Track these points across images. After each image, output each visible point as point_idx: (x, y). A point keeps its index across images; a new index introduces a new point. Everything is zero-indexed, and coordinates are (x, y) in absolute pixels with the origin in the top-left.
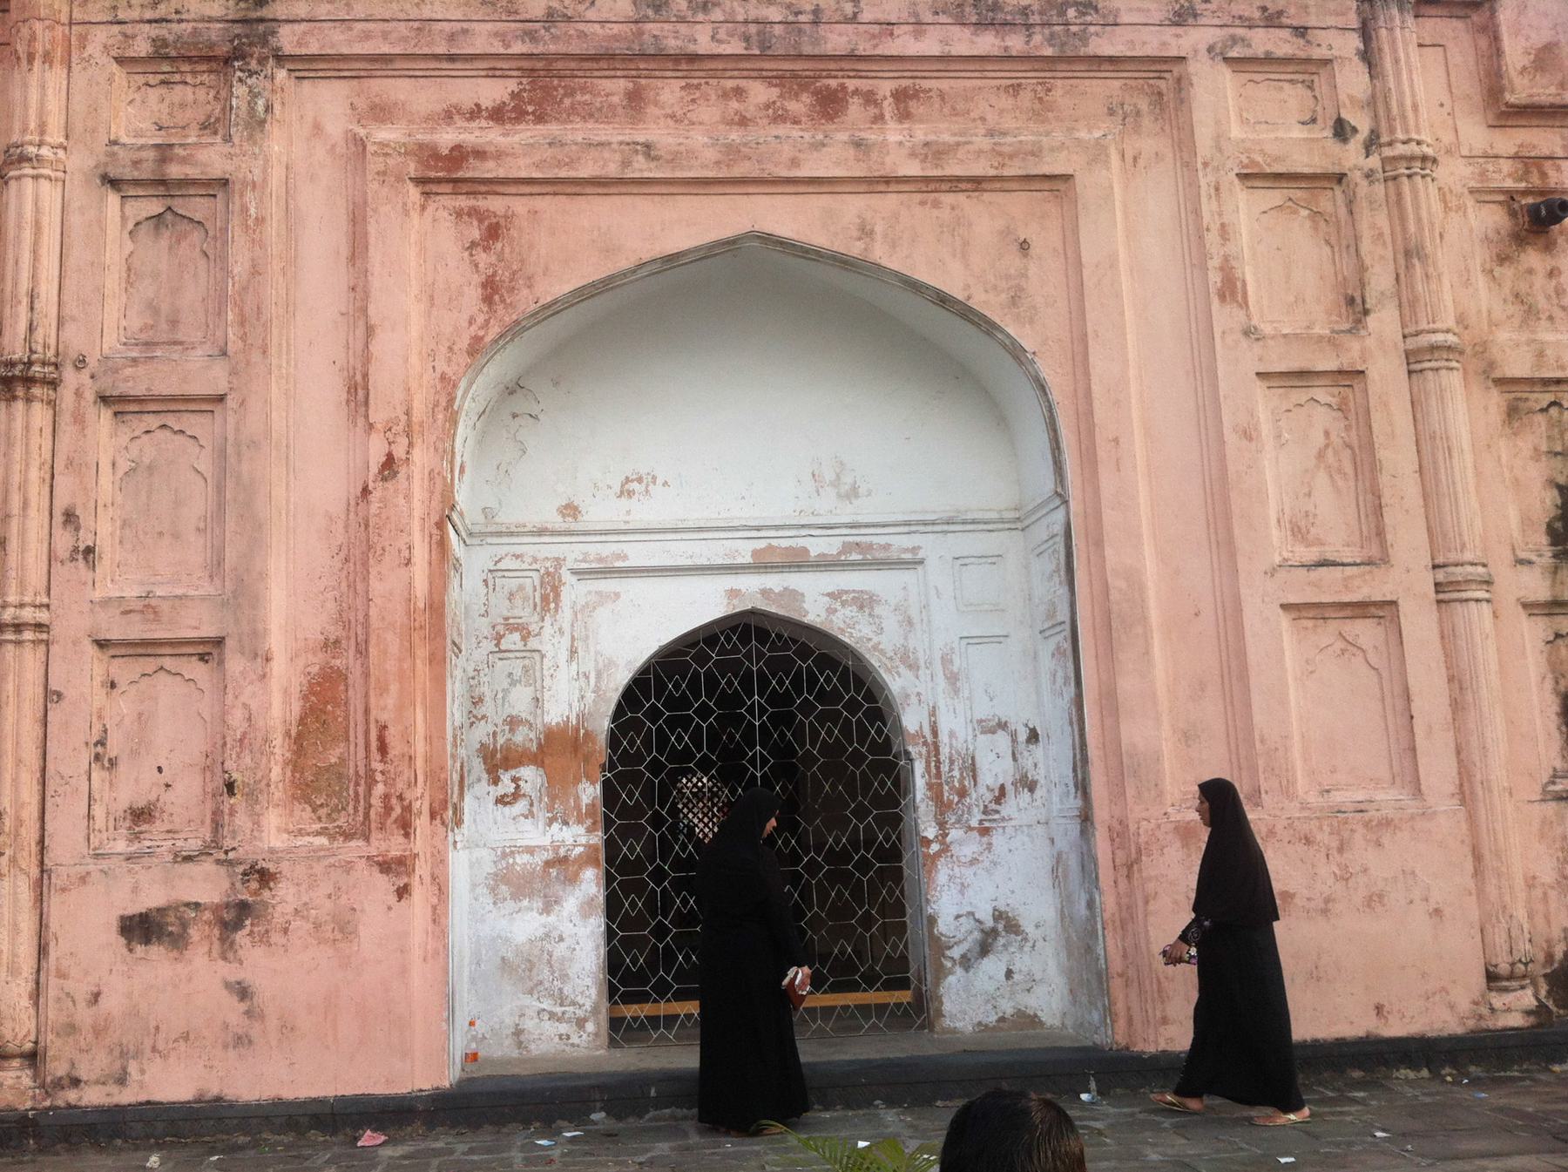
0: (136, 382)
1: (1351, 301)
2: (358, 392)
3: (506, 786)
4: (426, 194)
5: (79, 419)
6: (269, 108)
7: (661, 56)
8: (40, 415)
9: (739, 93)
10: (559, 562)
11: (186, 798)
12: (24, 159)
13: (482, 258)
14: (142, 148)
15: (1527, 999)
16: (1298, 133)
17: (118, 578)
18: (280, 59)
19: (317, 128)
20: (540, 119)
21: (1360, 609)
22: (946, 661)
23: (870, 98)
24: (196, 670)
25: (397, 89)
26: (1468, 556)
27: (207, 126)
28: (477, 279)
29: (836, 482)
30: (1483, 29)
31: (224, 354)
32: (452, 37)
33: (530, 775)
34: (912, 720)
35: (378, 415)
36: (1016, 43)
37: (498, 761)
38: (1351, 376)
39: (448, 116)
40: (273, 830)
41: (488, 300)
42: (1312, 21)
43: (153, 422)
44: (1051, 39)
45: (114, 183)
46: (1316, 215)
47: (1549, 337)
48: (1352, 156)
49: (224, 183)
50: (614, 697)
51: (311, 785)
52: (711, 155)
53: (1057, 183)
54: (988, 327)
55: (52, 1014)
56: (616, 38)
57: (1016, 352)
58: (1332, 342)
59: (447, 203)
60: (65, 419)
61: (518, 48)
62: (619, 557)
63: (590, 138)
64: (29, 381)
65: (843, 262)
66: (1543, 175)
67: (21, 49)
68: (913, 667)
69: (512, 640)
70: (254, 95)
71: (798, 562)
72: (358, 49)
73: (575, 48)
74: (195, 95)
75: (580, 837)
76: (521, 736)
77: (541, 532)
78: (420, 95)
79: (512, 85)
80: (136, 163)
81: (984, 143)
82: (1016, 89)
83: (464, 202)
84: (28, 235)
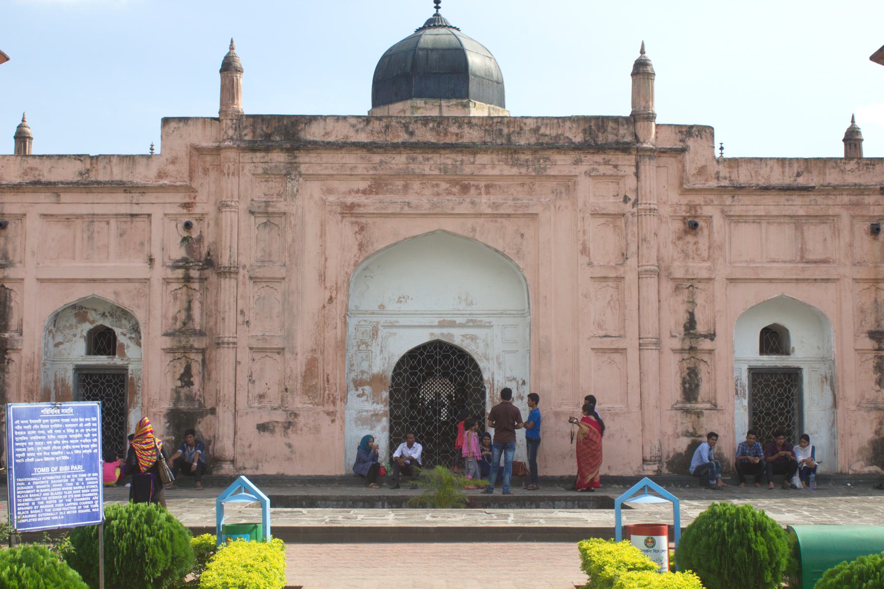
0: (260, 273)
1: (623, 255)
2: (322, 277)
3: (360, 391)
4: (343, 217)
5: (244, 284)
6: (297, 191)
7: (414, 174)
8: (233, 282)
9: (437, 185)
10: (378, 323)
11: (274, 393)
12: (227, 206)
13: (359, 237)
14: (261, 202)
15: (655, 467)
16: (612, 200)
17: (257, 330)
18: (300, 175)
19: (311, 196)
20: (377, 193)
21: (616, 350)
22: (498, 358)
23: (477, 187)
24: (276, 356)
25: (335, 184)
26: (650, 336)
27: (279, 195)
28: (357, 243)
29: (466, 300)
30: (681, 162)
31: (285, 265)
32: (351, 169)
33: (368, 389)
34: (486, 376)
35: (328, 285)
36: (523, 171)
37: (358, 384)
38: (619, 279)
39: (350, 192)
40: (298, 402)
41: (360, 249)
42: (620, 163)
43: (264, 284)
44: (534, 170)
45: (252, 213)
46: (615, 226)
47: (691, 264)
48: (628, 208)
49: (285, 214)
50: (394, 365)
51: (309, 390)
52: (428, 206)
53: (534, 216)
54: (511, 260)
55: (238, 450)
56: (400, 169)
57: (518, 267)
58: (615, 268)
59: (348, 219)
60: (240, 283)
61: (371, 172)
62: (396, 322)
63: (391, 200)
64: (230, 273)
65: (467, 238)
66: (696, 211)
67: (226, 171)
68: (488, 360)
69: (363, 347)
70: (293, 186)
71: (453, 324)
72: (323, 172)
73: (388, 172)
74: (275, 185)
75: (382, 408)
76: (365, 376)
77: (373, 313)
78: (342, 186)
79: (369, 183)
80: (259, 207)
81: (511, 203)
82: (523, 185)
83: (354, 219)
84: (229, 229)
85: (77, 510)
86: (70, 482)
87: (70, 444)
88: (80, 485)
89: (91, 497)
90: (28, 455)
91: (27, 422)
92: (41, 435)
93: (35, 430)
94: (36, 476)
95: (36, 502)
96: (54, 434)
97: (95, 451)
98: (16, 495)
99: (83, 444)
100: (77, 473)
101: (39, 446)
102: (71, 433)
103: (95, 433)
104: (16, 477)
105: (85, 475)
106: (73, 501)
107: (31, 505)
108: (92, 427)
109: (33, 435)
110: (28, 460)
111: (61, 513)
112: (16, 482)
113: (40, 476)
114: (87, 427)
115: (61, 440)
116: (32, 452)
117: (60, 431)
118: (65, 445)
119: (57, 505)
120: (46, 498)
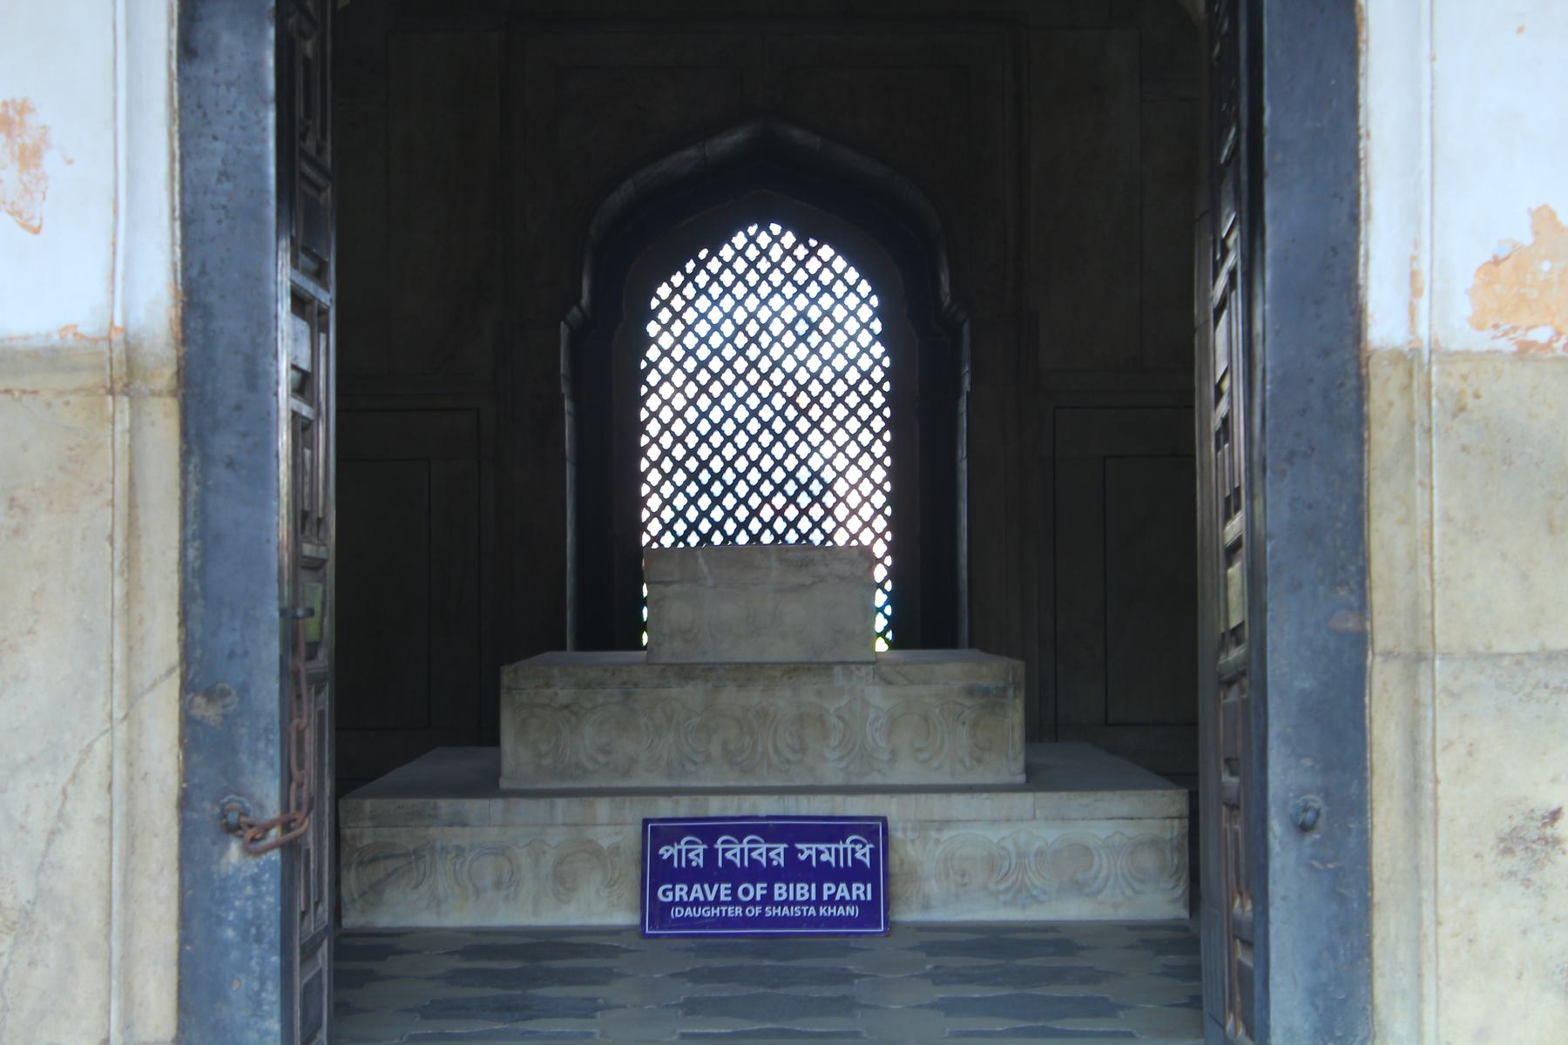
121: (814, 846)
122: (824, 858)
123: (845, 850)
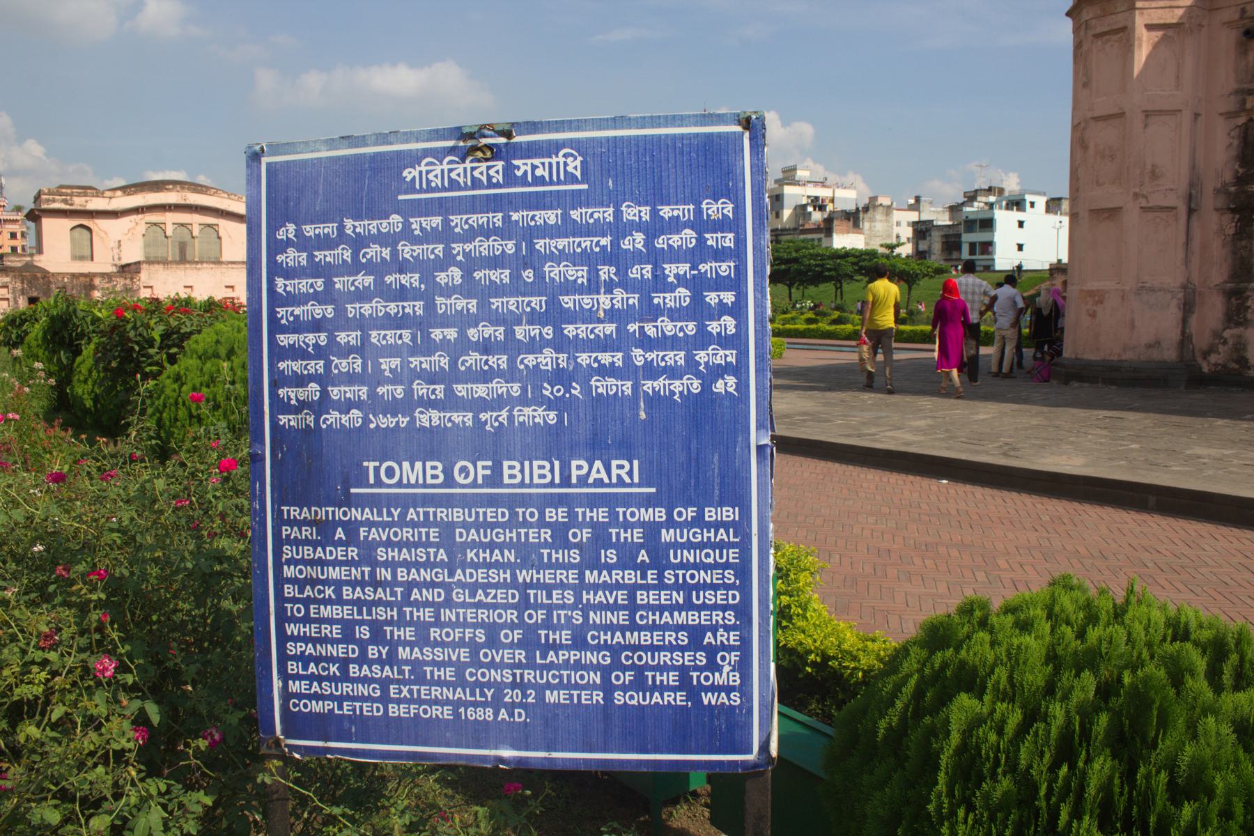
85: (608, 688)
86: (560, 538)
87: (560, 343)
88: (627, 560)
89: (696, 634)
90: (335, 393)
91: (329, 229)
92: (402, 294)
93: (370, 268)
94: (373, 502)
95: (378, 635)
96: (468, 288)
97: (725, 385)
98: (280, 581)
99: (647, 343)
100: (610, 501)
101: (392, 351)
102: (570, 287)
103: (719, 284)
104: (279, 501)
105: (659, 514)
106: (579, 643)
107: (348, 636)
108: (699, 253)
109: (362, 296)
110: (332, 417)
111: (511, 696)
112: (279, 521)
113: (392, 501)
114: (675, 255)
115: (508, 321)
116: (351, 378)
117: (502, 276)
118: (534, 346)
119: (486, 655)
120: (426, 615)
121: (529, 162)
122: (539, 172)
123: (558, 163)
